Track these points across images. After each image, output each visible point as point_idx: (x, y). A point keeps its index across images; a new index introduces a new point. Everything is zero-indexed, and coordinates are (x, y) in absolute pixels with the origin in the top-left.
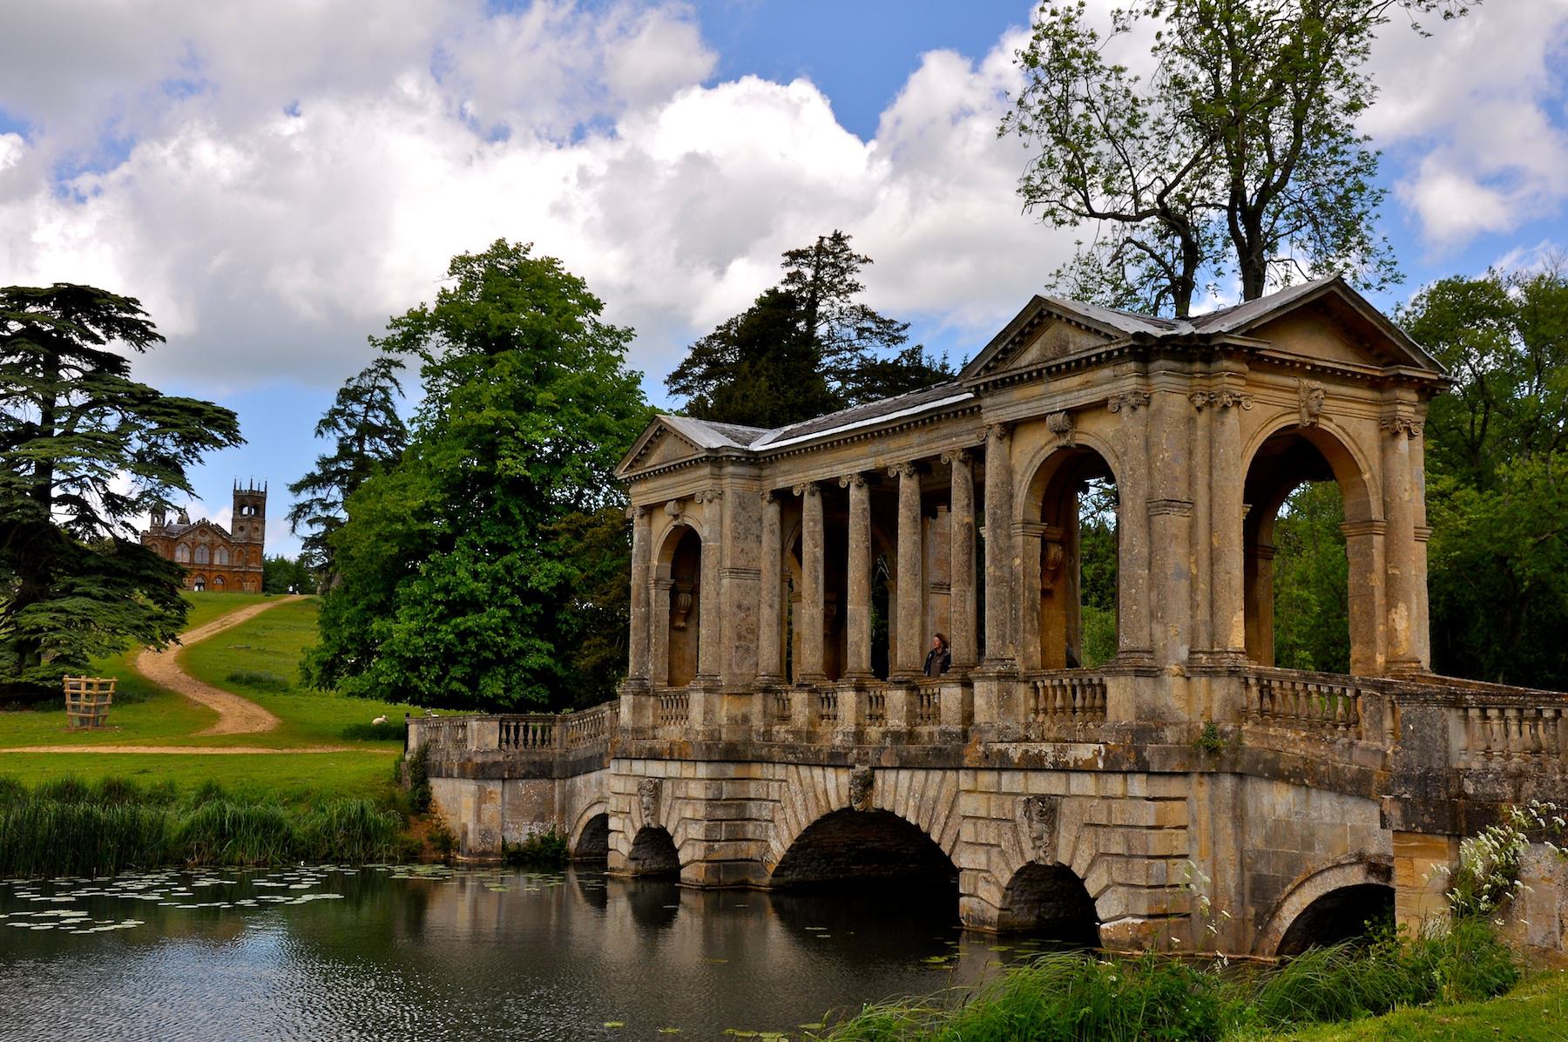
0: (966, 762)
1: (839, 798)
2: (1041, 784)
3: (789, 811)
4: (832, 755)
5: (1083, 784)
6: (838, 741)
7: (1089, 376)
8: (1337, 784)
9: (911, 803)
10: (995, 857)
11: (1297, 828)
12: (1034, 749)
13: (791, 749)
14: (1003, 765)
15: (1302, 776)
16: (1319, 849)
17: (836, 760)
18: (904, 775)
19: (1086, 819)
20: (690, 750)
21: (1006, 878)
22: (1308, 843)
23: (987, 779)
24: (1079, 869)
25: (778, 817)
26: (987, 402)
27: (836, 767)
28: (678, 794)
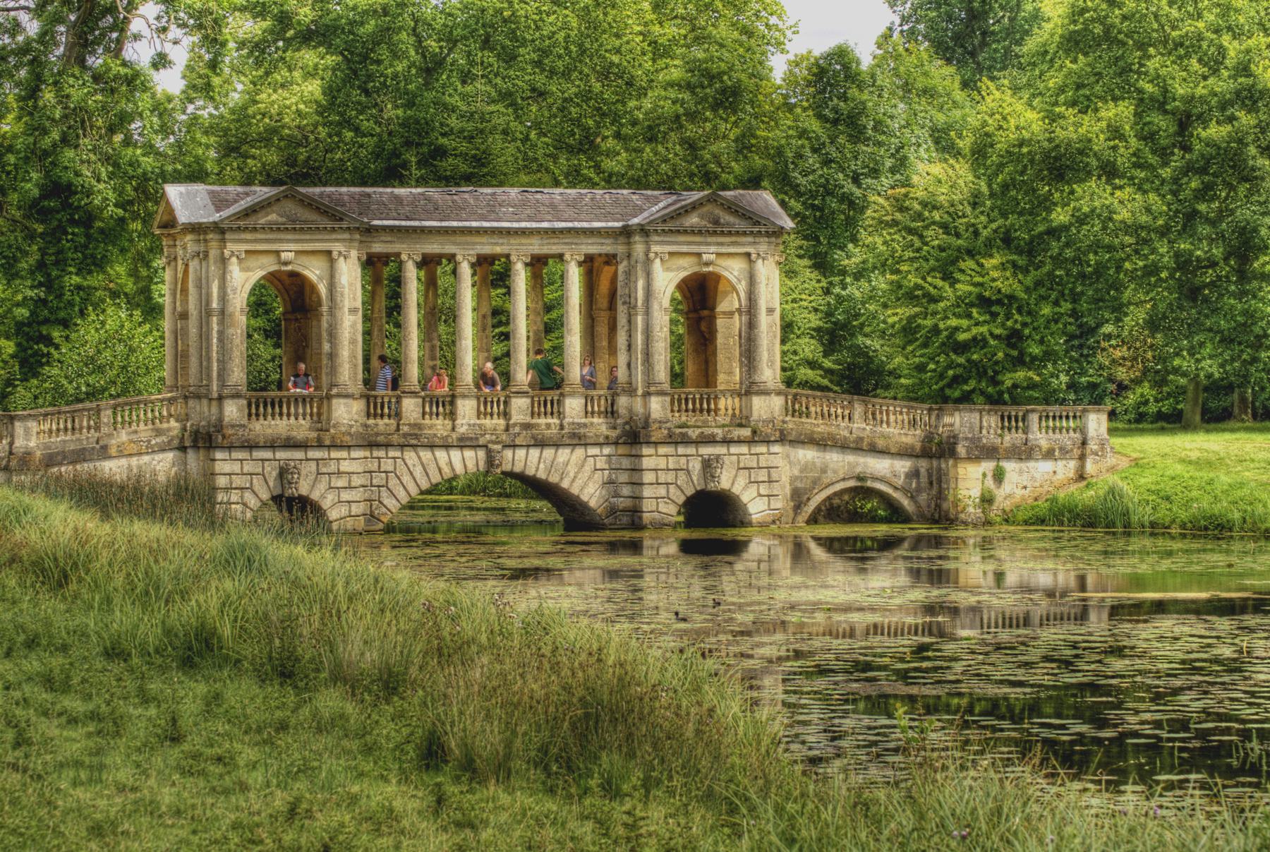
0: (653, 439)
1: (465, 466)
2: (706, 451)
3: (406, 479)
4: (461, 439)
5: (744, 449)
6: (462, 430)
7: (733, 239)
8: (844, 446)
9: (542, 466)
10: (672, 489)
11: (818, 465)
12: (708, 431)
13: (417, 436)
14: (686, 441)
15: (821, 443)
16: (830, 474)
17: (464, 443)
18: (534, 453)
19: (742, 465)
20: (347, 438)
21: (681, 500)
22: (824, 471)
23: (663, 450)
24: (736, 490)
25: (393, 482)
26: (656, 238)
27: (461, 447)
28: (324, 470)
